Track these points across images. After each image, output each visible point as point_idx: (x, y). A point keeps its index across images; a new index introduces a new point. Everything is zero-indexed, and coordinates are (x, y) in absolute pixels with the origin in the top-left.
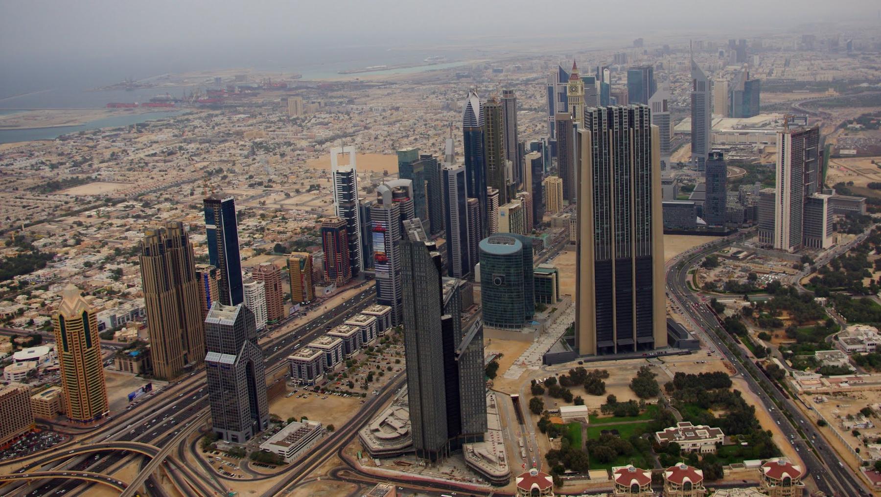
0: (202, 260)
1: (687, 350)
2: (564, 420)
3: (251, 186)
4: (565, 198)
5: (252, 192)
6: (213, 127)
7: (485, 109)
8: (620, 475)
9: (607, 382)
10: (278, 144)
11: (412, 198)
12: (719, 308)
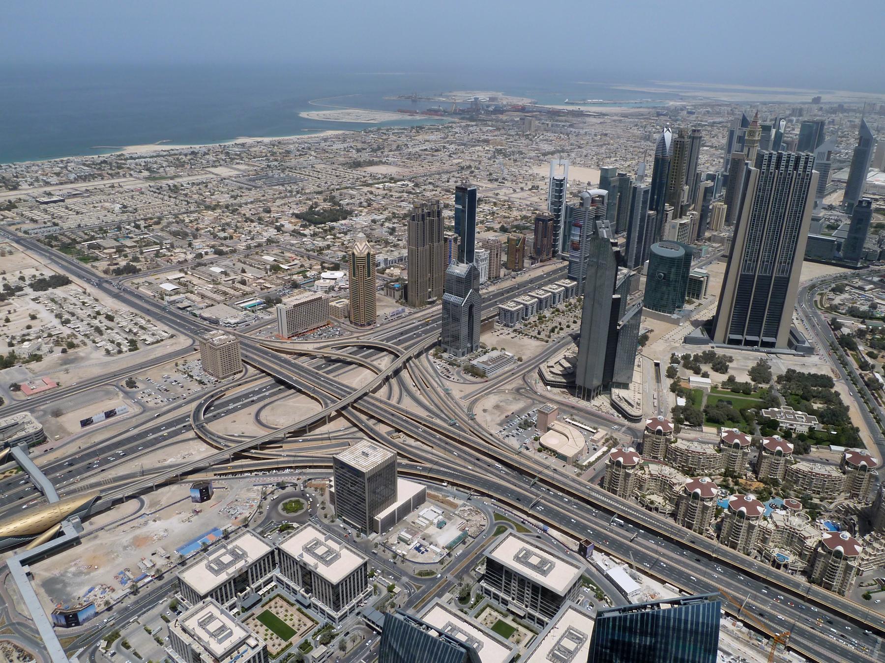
1: (802, 353)
2: (692, 385)
4: (726, 221)
5: (490, 185)
6: (469, 135)
7: (675, 143)
8: (727, 434)
9: (730, 365)
10: (513, 152)
11: (605, 205)
12: (836, 326)
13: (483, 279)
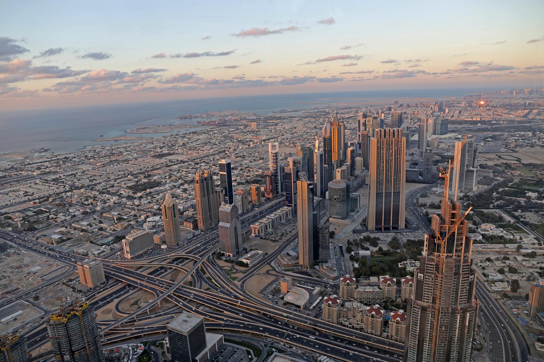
0: (218, 186)
3: (237, 157)
9: (379, 242)
13: (240, 212)
